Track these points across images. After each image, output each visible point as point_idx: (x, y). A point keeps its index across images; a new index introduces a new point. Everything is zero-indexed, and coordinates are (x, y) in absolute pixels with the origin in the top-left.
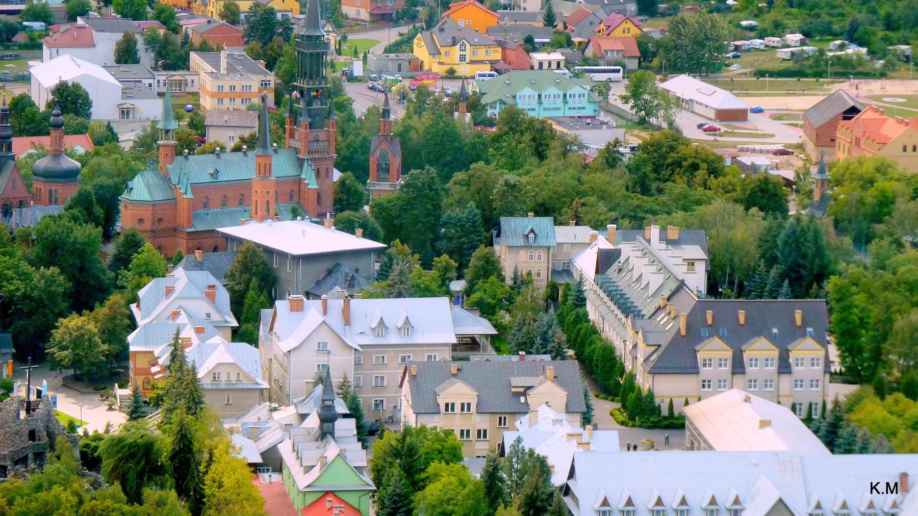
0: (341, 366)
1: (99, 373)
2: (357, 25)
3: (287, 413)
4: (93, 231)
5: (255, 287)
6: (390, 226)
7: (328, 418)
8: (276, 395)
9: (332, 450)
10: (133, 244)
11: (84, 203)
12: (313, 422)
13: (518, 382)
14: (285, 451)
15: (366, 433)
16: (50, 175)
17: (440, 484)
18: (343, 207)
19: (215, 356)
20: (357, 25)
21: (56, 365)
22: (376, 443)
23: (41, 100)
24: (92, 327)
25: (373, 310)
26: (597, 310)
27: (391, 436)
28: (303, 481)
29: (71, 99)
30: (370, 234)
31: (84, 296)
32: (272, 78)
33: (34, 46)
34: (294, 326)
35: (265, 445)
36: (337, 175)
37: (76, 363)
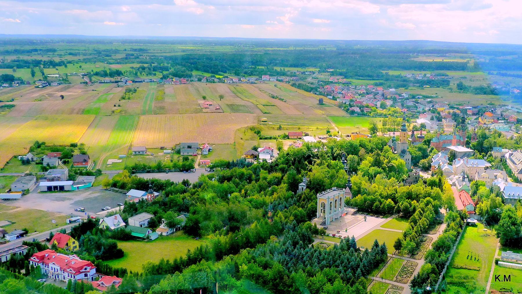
0: (466, 170)
1: (426, 169)
2: (470, 115)
3: (457, 177)
4: (427, 147)
5: (453, 157)
6: (474, 148)
7: (464, 178)
8: (455, 174)
9: (464, 183)
10: (433, 149)
11: (425, 142)
12: (461, 178)
13: (495, 174)
14: (456, 183)
15: (470, 181)
16: (420, 137)
17: (483, 190)
18: (467, 144)
19: (446, 167)
20: (470, 115)
21: (420, 167)
22: (472, 183)
23: (419, 126)
24: (426, 162)
25: (472, 161)
26: (509, 162)
27: (474, 182)
28: (459, 188)
29: (423, 126)
30: (471, 148)
31: (425, 156)
32: (455, 123)
33: (418, 117)
34: (459, 163)
35: (453, 181)
36: (466, 139)
37: (423, 167)
